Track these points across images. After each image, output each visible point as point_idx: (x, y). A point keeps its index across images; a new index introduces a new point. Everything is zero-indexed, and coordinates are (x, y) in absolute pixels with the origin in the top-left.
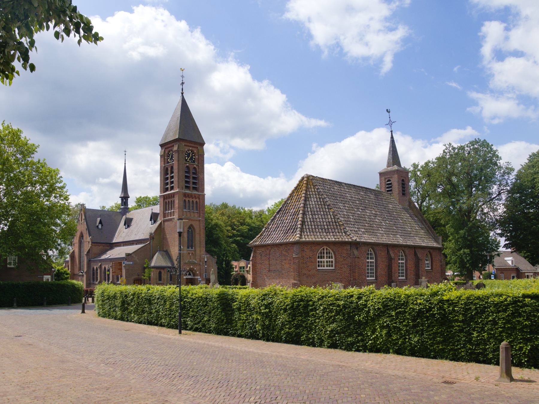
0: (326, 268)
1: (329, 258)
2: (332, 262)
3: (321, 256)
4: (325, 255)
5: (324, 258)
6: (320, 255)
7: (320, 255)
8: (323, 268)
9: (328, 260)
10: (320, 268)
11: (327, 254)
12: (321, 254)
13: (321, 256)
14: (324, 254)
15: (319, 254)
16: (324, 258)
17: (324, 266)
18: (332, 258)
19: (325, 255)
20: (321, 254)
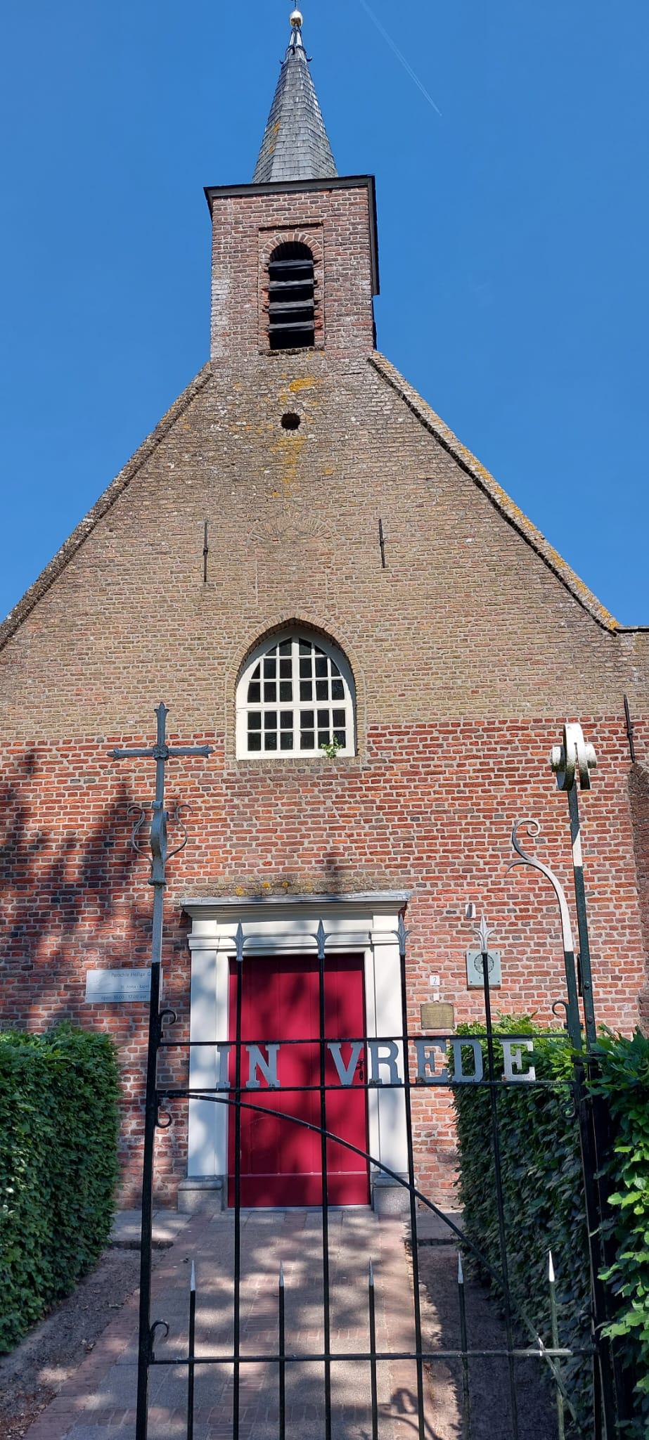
0: (297, 752)
1: (322, 696)
2: (340, 716)
3: (270, 688)
4: (296, 680)
5: (287, 696)
6: (262, 680)
7: (262, 680)
8: (279, 754)
9: (315, 705)
10: (263, 754)
11: (305, 668)
12: (270, 672)
13: (270, 688)
14: (286, 669)
15: (256, 674)
16: (287, 696)
17: (287, 743)
18: (338, 695)
19: (296, 680)
20: (270, 672)
